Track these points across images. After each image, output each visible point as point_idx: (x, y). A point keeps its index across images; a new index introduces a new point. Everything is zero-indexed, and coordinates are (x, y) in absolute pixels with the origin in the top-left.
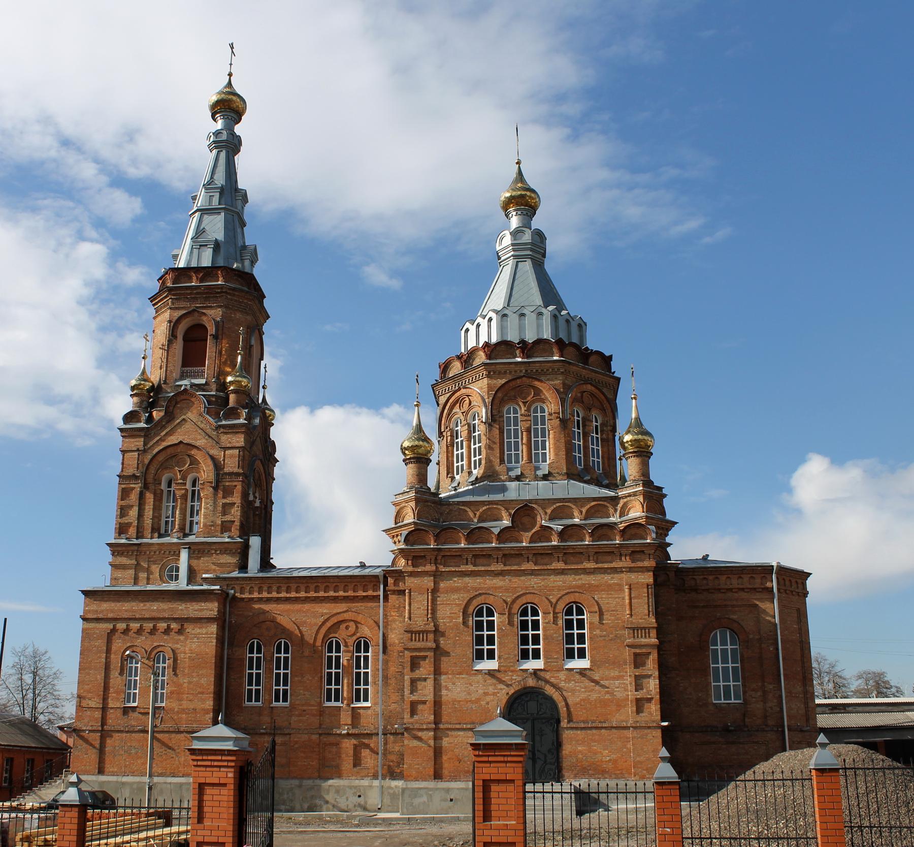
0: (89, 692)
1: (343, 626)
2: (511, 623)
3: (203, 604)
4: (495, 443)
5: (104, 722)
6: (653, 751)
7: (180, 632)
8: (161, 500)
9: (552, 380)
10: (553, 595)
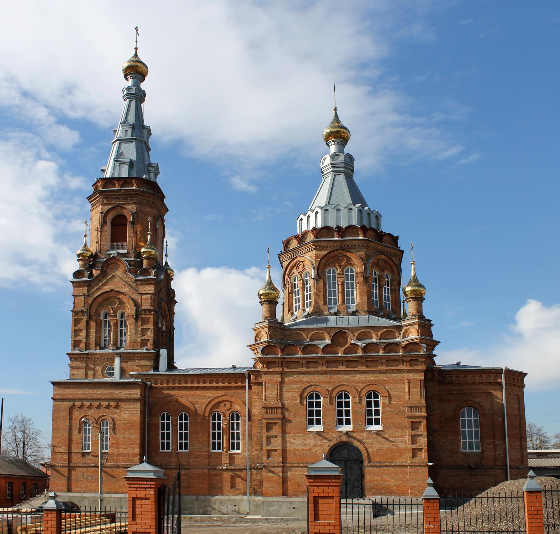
0: (59, 443)
1: (222, 404)
2: (331, 403)
3: (131, 391)
4: (320, 292)
5: (70, 461)
6: (423, 480)
7: (117, 407)
8: (100, 326)
9: (358, 252)
10: (359, 386)
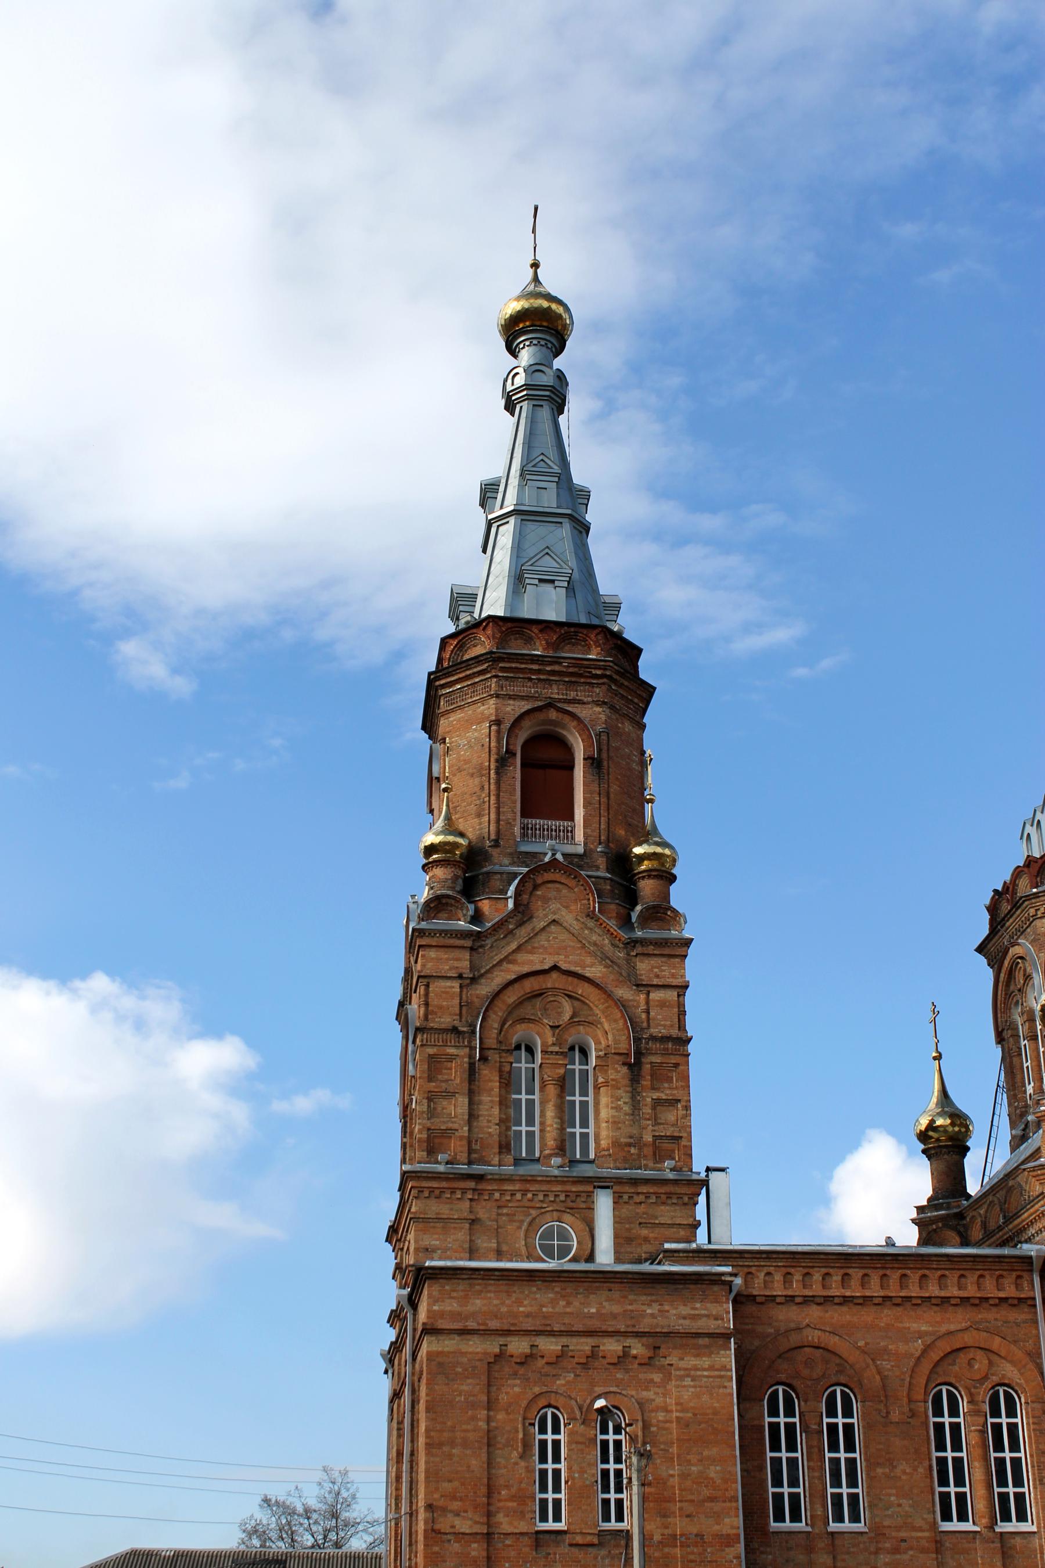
3: (698, 1305)
